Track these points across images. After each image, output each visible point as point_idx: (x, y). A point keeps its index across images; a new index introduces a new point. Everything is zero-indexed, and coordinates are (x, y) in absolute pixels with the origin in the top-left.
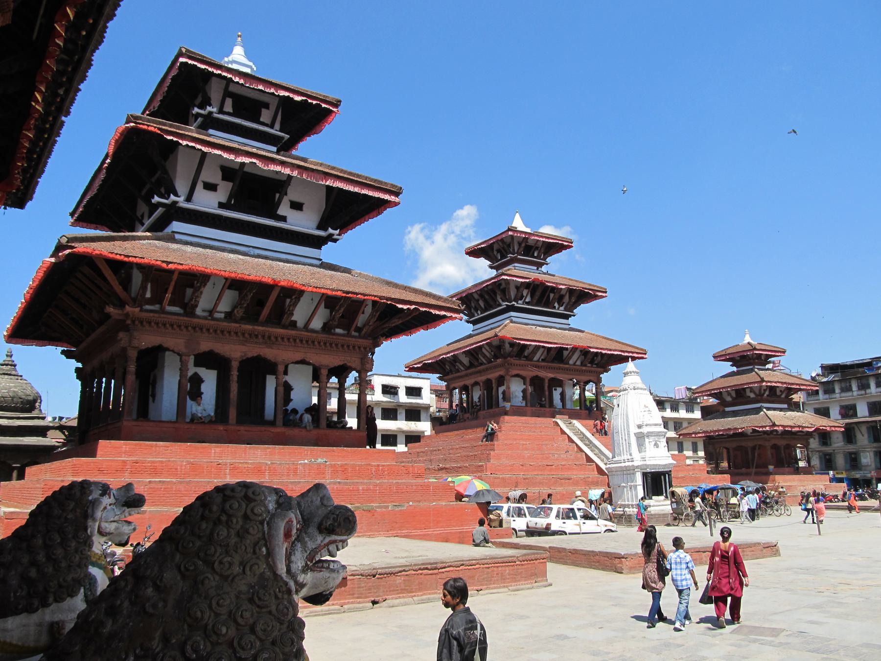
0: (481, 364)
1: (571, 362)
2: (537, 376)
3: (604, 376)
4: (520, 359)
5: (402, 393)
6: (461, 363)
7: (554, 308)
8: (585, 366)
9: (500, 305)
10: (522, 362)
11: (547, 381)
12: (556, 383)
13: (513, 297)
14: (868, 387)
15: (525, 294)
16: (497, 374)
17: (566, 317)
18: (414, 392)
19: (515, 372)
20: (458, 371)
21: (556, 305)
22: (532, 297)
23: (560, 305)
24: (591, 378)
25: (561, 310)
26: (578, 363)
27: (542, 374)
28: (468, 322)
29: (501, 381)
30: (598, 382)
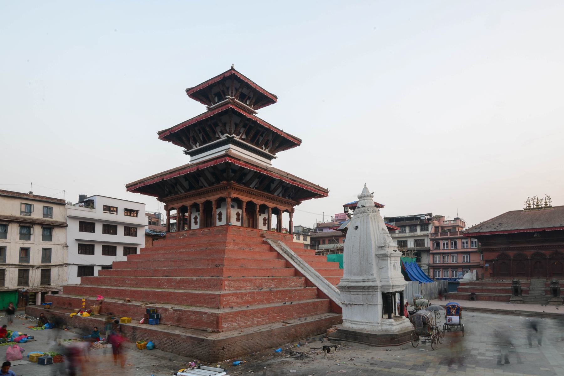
0: (202, 187)
1: (276, 194)
2: (251, 201)
3: (296, 208)
4: (239, 184)
5: (121, 212)
6: (182, 186)
7: (262, 149)
8: (285, 198)
9: (219, 138)
10: (242, 186)
11: (258, 207)
12: (263, 209)
13: (233, 131)
14: (416, 231)
15: (242, 131)
16: (217, 196)
17: (270, 158)
18: (130, 212)
19: (234, 195)
20: (176, 193)
21: (263, 147)
22: (247, 136)
23: (266, 148)
24: (288, 209)
25: (267, 152)
26: (281, 195)
27: (255, 201)
28: (186, 153)
29: (221, 202)
30: (291, 212)
